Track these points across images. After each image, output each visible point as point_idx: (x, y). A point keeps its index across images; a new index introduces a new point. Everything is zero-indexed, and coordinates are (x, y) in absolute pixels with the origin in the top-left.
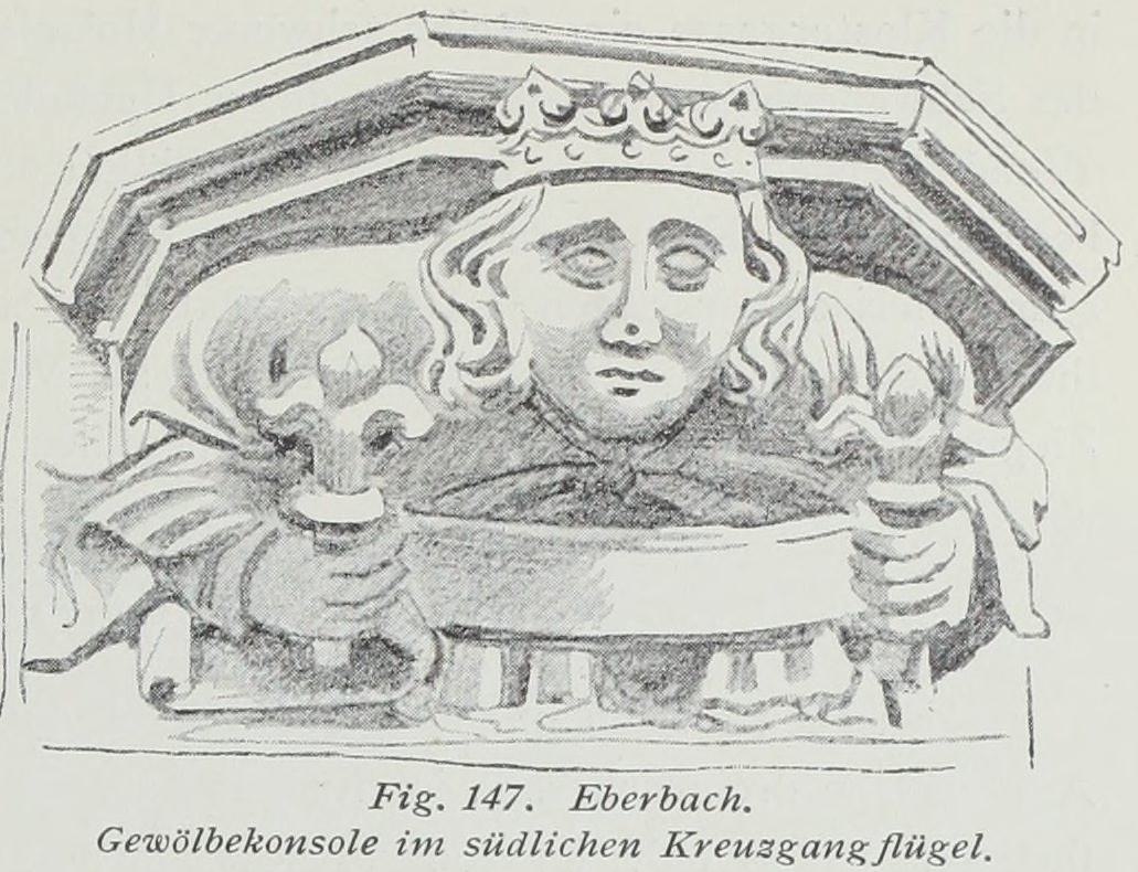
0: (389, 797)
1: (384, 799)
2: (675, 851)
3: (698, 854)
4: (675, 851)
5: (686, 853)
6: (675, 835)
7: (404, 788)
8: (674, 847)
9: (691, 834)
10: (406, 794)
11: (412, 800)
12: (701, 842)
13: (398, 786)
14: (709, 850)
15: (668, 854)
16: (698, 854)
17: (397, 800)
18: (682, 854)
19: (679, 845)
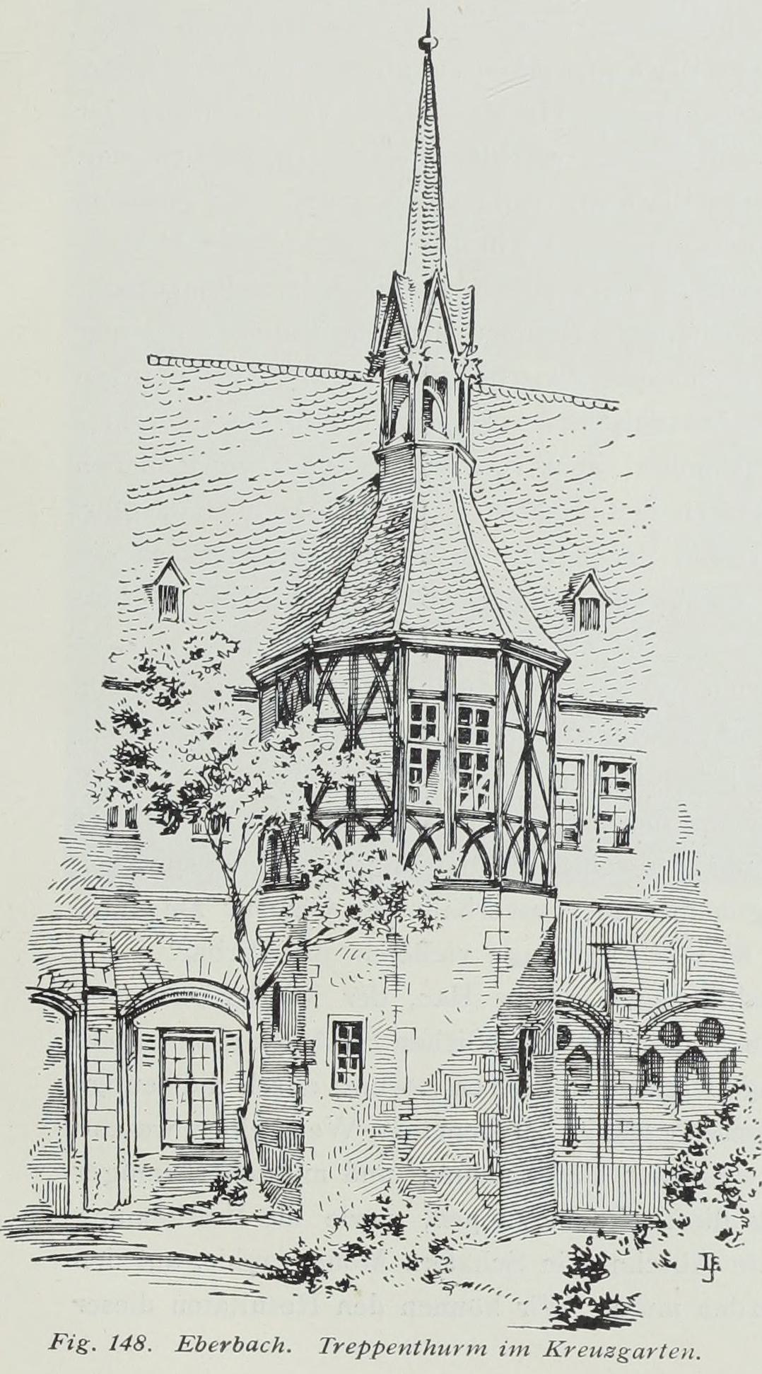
0: (61, 1342)
1: (58, 1343)
2: (552, 1353)
3: (566, 1355)
4: (552, 1353)
5: (559, 1354)
6: (552, 1343)
7: (70, 1337)
8: (552, 1350)
9: (562, 1342)
10: (72, 1341)
11: (75, 1345)
12: (569, 1347)
13: (67, 1335)
14: (574, 1353)
15: (548, 1355)
16: (566, 1355)
17: (65, 1343)
18: (557, 1355)
19: (555, 1349)
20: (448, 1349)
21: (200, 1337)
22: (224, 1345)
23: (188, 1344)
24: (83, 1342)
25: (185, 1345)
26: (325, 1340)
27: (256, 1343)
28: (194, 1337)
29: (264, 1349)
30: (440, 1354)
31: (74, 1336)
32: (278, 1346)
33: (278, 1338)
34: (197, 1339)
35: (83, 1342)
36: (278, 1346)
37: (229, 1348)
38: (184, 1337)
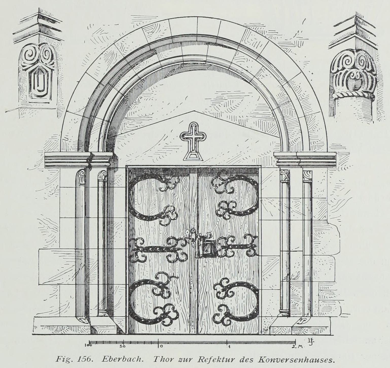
0: (60, 359)
4: (261, 361)
6: (261, 357)
8: (261, 360)
9: (265, 357)
10: (64, 358)
13: (62, 356)
15: (260, 362)
18: (263, 362)
19: (262, 360)
20: (187, 360)
21: (111, 356)
22: (119, 359)
23: (106, 359)
24: (68, 359)
25: (105, 359)
26: (156, 357)
27: (131, 359)
28: (108, 356)
29: (133, 361)
30: (184, 361)
31: (65, 357)
32: (139, 359)
33: (139, 357)
34: (110, 357)
35: (68, 359)
36: (139, 359)
37: (121, 360)
38: (105, 356)
